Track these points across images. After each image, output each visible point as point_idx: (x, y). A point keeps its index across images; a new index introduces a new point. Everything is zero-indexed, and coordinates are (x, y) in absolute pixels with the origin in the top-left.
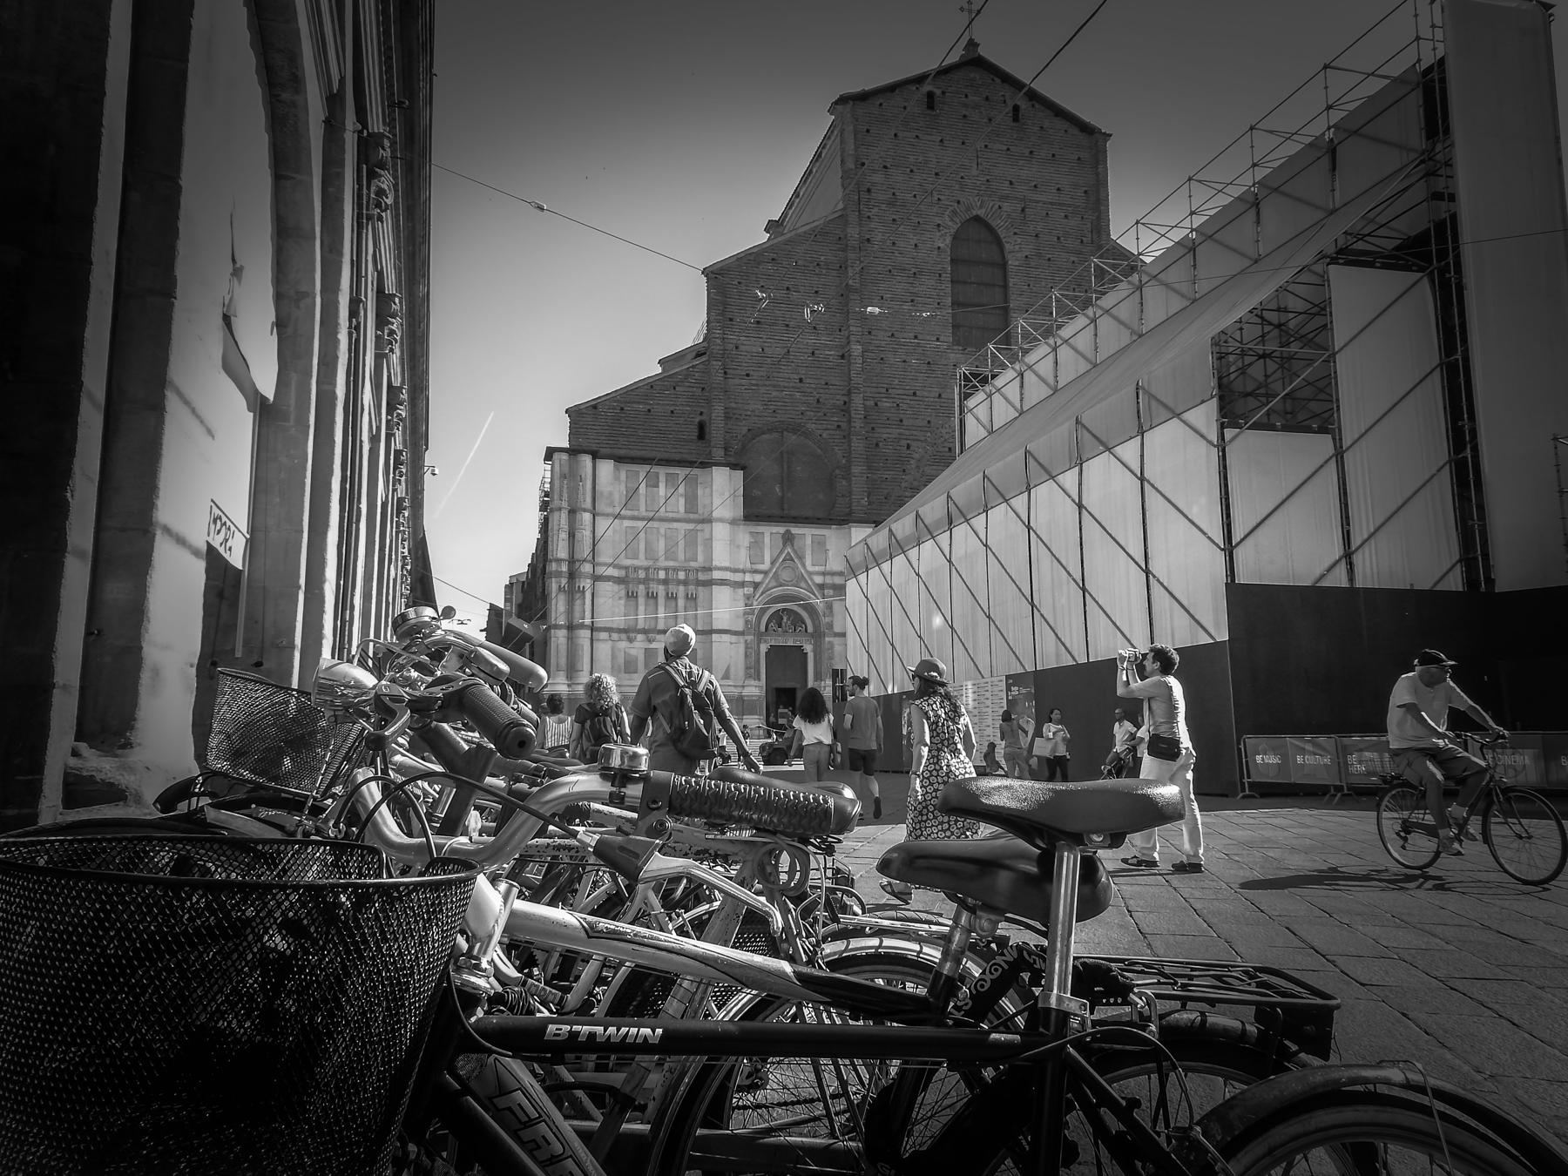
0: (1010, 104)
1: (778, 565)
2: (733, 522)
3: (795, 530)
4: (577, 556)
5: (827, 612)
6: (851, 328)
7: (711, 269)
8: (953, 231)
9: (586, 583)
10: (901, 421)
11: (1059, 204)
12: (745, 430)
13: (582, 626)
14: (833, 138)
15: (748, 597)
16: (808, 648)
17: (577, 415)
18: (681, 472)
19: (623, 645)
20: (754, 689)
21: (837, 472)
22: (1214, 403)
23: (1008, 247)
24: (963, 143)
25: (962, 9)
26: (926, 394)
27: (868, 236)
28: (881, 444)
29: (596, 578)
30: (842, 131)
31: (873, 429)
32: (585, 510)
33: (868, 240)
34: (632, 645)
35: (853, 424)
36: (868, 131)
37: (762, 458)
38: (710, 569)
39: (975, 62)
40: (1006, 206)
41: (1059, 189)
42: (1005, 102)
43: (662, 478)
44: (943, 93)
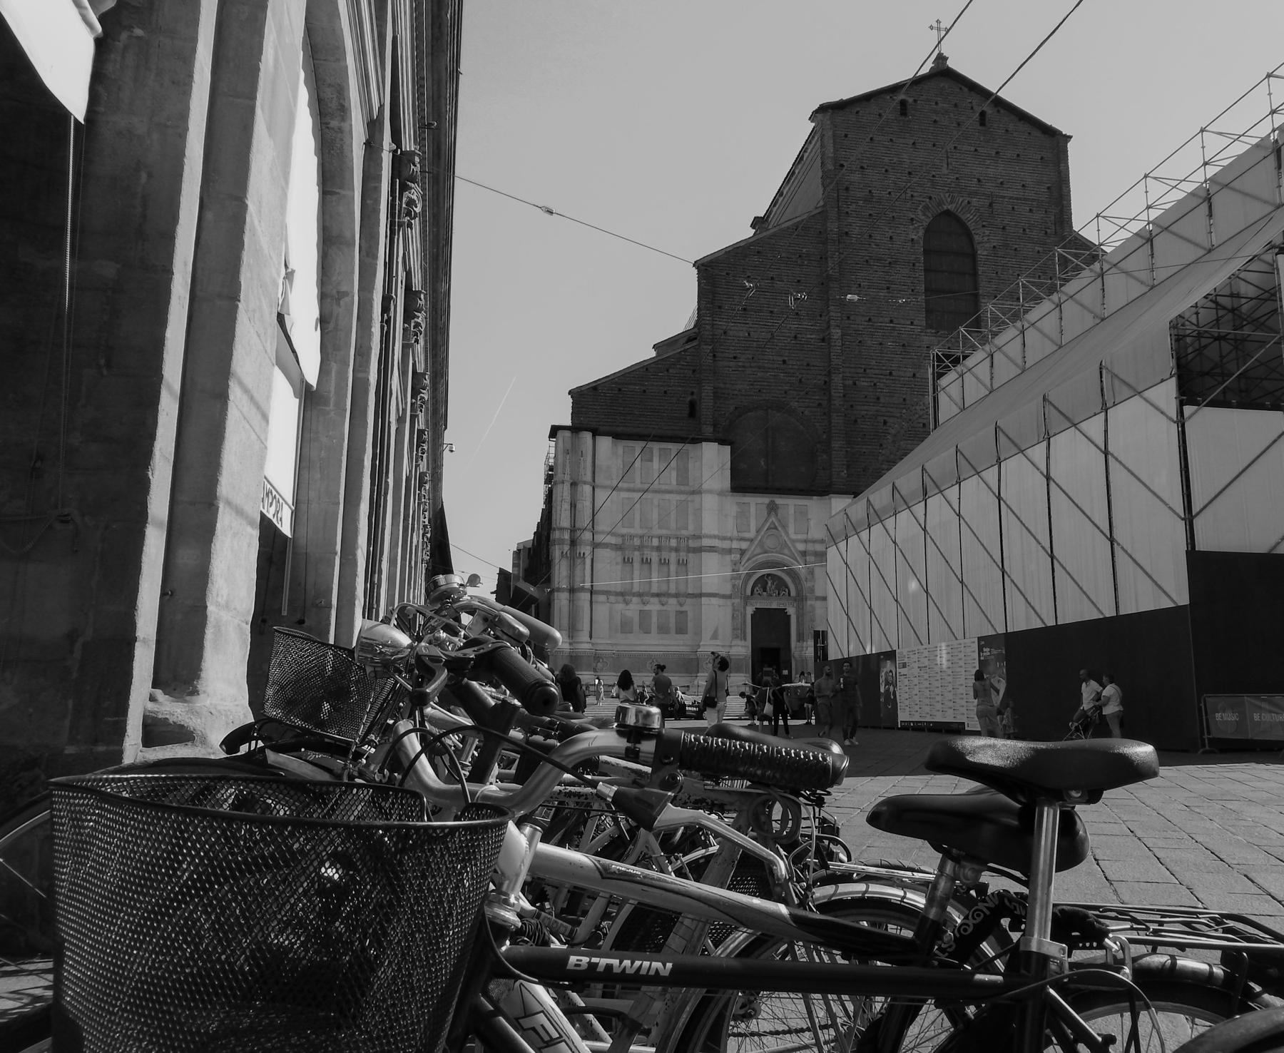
0: (978, 110)
1: (763, 533)
2: (721, 493)
4: (577, 526)
6: (832, 314)
7: (701, 262)
8: (925, 224)
9: (587, 550)
10: (878, 399)
11: (1025, 199)
12: (732, 408)
13: (583, 589)
14: (813, 142)
16: (791, 611)
17: (581, 397)
18: (674, 447)
19: (621, 606)
21: (818, 446)
22: (1174, 380)
23: (976, 237)
24: (934, 145)
25: (931, 28)
26: (902, 374)
29: (595, 546)
30: (822, 136)
31: (852, 406)
32: (585, 483)
33: (847, 233)
34: (628, 607)
35: (832, 402)
36: (846, 136)
38: (700, 537)
39: (942, 74)
41: (1023, 186)
42: (972, 108)
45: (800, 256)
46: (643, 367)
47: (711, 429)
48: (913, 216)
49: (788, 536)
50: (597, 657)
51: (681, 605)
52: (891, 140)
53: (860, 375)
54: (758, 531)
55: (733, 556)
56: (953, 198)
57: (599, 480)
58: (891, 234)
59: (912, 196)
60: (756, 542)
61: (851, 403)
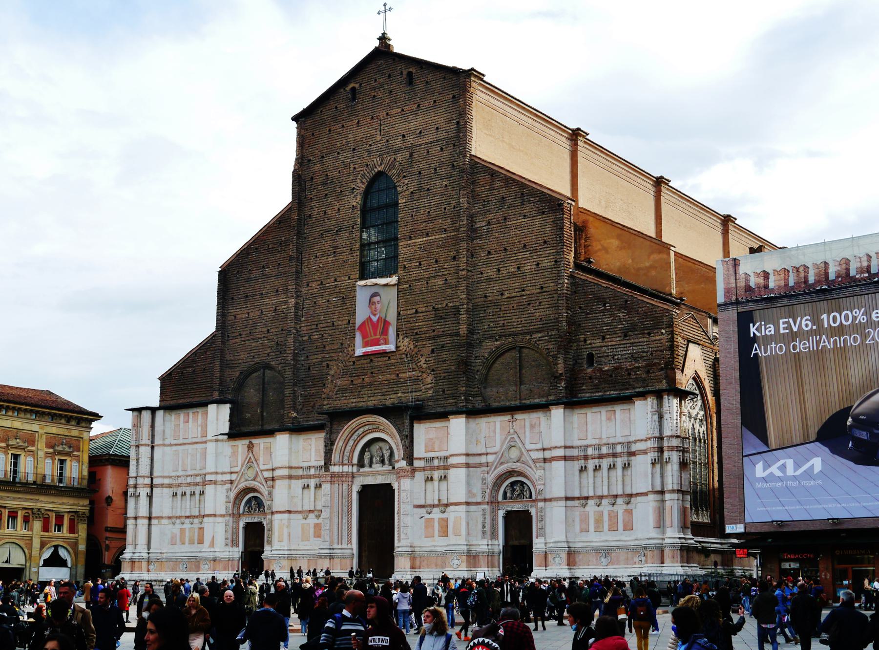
0: (405, 73)
1: (244, 466)
3: (254, 441)
5: (269, 498)
8: (361, 189)
10: (325, 347)
11: (437, 141)
12: (238, 374)
16: (265, 523)
17: (167, 380)
18: (200, 410)
19: (171, 526)
20: (227, 554)
23: (399, 189)
24: (372, 118)
25: (379, 13)
27: (309, 213)
28: (311, 368)
31: (307, 357)
32: (142, 445)
33: (310, 215)
36: (313, 134)
37: (252, 390)
40: (399, 157)
41: (437, 128)
42: (402, 73)
44: (361, 84)
45: (281, 244)
46: (193, 353)
47: (217, 393)
48: (354, 186)
49: (259, 469)
51: (201, 523)
52: (343, 126)
53: (314, 330)
54: (242, 465)
55: (227, 485)
56: (382, 160)
57: (156, 442)
58: (338, 206)
60: (241, 474)
61: (306, 355)
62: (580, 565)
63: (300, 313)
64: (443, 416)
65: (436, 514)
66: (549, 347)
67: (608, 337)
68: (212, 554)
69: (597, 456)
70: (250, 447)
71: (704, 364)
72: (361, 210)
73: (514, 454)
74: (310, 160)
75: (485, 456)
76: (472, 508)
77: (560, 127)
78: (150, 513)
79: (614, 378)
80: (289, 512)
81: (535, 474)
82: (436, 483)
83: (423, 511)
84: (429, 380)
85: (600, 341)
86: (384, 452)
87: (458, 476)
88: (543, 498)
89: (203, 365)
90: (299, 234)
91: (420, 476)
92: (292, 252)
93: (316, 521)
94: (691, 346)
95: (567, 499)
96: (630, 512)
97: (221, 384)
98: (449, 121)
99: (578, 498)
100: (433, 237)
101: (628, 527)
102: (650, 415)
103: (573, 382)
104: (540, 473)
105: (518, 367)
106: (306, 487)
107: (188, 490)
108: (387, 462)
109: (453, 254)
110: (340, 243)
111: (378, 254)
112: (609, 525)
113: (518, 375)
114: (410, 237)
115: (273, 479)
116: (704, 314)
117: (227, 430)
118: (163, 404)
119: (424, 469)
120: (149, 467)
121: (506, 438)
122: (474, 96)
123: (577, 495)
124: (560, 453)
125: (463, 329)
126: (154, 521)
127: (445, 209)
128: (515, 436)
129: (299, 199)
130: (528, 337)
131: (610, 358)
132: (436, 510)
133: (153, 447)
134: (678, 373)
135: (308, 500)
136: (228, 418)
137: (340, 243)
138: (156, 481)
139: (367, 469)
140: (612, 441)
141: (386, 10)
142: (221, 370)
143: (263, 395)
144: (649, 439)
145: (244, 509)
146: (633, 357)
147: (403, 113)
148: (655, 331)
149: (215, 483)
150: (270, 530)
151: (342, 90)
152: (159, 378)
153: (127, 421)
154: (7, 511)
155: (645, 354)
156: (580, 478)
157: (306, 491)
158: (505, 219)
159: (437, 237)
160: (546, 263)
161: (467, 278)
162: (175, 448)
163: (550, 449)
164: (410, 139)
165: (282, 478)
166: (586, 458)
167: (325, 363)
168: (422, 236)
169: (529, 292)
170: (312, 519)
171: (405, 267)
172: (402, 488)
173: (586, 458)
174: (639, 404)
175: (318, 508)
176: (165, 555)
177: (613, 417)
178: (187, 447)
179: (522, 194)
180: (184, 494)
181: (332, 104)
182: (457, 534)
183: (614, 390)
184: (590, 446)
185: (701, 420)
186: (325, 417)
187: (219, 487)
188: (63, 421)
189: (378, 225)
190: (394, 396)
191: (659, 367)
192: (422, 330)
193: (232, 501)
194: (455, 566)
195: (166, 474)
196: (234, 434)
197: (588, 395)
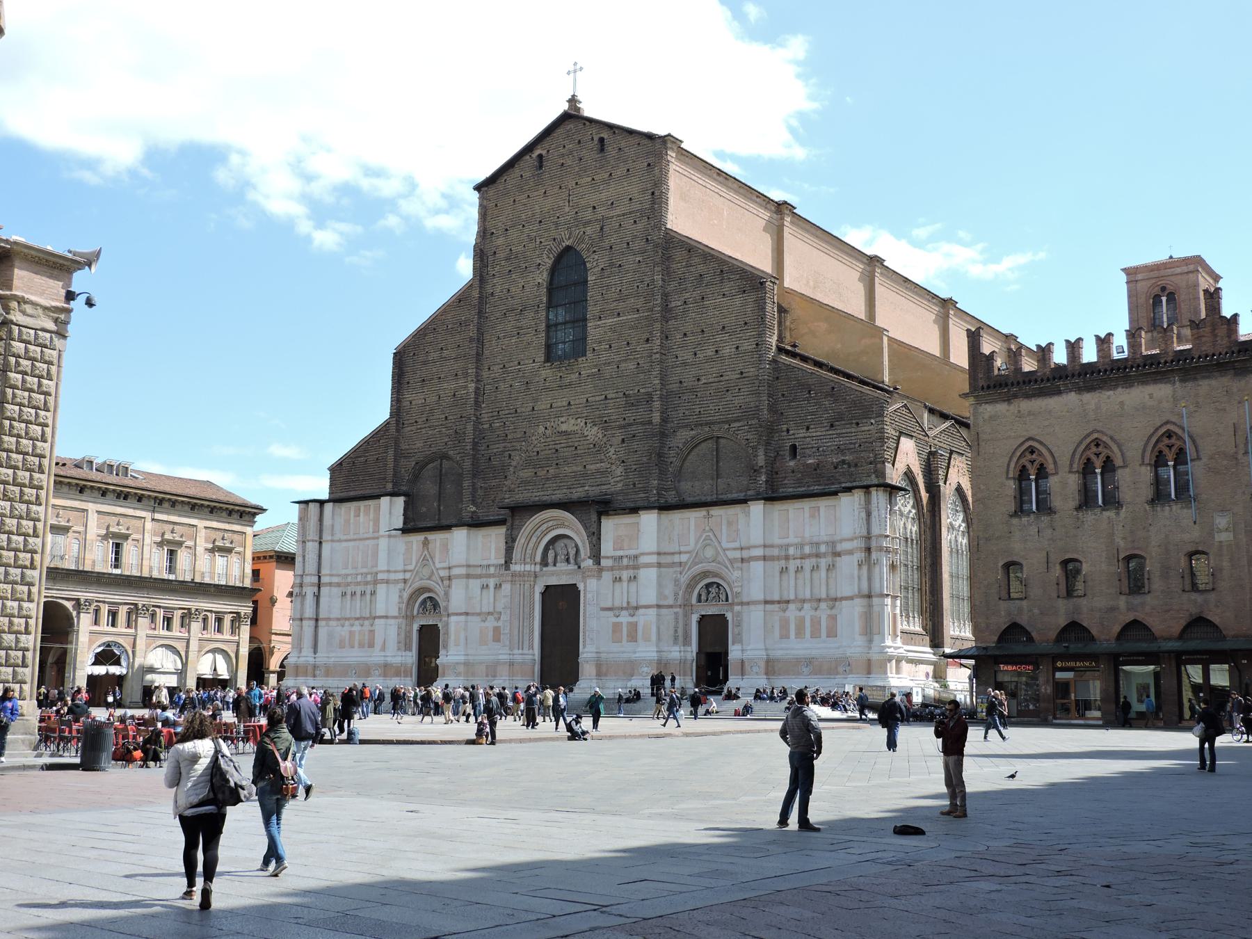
0: (596, 138)
3: (432, 536)
8: (549, 265)
11: (630, 213)
15: (400, 592)
16: (440, 625)
18: (371, 503)
19: (339, 628)
20: (400, 658)
23: (588, 265)
24: (560, 187)
26: (523, 409)
32: (308, 541)
36: (496, 205)
40: (589, 230)
41: (631, 199)
42: (592, 139)
43: (362, 509)
44: (548, 151)
50: (315, 667)
51: (372, 625)
54: (417, 563)
57: (326, 536)
58: (523, 284)
59: (541, 242)
62: (779, 674)
63: (481, 399)
64: (634, 510)
65: (624, 618)
66: (748, 437)
67: (812, 427)
68: (382, 658)
69: (799, 556)
70: (426, 543)
71: (917, 458)
72: (547, 288)
73: (709, 553)
74: (493, 233)
75: (677, 556)
76: (664, 611)
77: (765, 200)
78: (317, 613)
79: (818, 471)
80: (467, 614)
81: (734, 575)
82: (625, 584)
83: (610, 613)
84: (619, 471)
85: (804, 431)
86: (570, 550)
87: (649, 576)
88: (739, 601)
89: (376, 454)
90: (481, 313)
91: (607, 576)
92: (472, 331)
93: (496, 624)
94: (903, 439)
95: (766, 602)
96: (833, 618)
97: (395, 475)
98: (644, 191)
99: (779, 602)
100: (625, 318)
101: (832, 633)
102: (856, 513)
103: (774, 476)
104: (737, 574)
105: (715, 460)
106: (485, 587)
107: (359, 589)
108: (572, 561)
109: (645, 336)
110: (523, 323)
111: (565, 336)
112: (812, 632)
113: (715, 468)
114: (600, 317)
115: (450, 578)
116: (919, 404)
117: (400, 525)
118: (332, 496)
119: (612, 569)
120: (316, 565)
121: (701, 536)
122: (670, 164)
123: (776, 598)
124: (759, 552)
125: (656, 417)
126: (321, 623)
127: (638, 287)
128: (710, 534)
129: (481, 276)
130: (727, 426)
131: (814, 449)
132: (624, 613)
133: (320, 543)
134: (888, 466)
135: (486, 601)
136: (402, 512)
137: (523, 323)
138: (324, 580)
139: (550, 568)
140: (815, 539)
141: (575, 70)
142: (395, 460)
143: (440, 487)
144: (856, 538)
145: (418, 611)
146: (840, 450)
147: (593, 182)
148: (865, 421)
149: (387, 582)
150: (447, 633)
151: (528, 157)
152: (328, 469)
153: (292, 515)
154: (162, 610)
155: (852, 446)
156: (781, 580)
157: (485, 591)
158: (703, 298)
159: (629, 317)
160: (747, 346)
161: (661, 362)
162: (344, 544)
163: (748, 548)
164: (601, 211)
165: (459, 577)
166: (787, 558)
167: (507, 453)
168: (612, 316)
169: (727, 378)
170: (491, 623)
171: (594, 350)
172: (588, 589)
173: (787, 558)
174: (845, 499)
175: (498, 610)
176: (333, 659)
177: (817, 514)
178: (358, 542)
179: (722, 271)
180: (353, 594)
181: (516, 172)
182: (647, 639)
183: (818, 485)
184: (792, 545)
185: (913, 519)
186: (507, 511)
187: (391, 586)
188: (224, 514)
189: (566, 304)
190: (581, 489)
191: (869, 460)
192: (612, 418)
193: (405, 601)
194: (644, 674)
195: (334, 572)
196: (405, 530)
197: (791, 490)
